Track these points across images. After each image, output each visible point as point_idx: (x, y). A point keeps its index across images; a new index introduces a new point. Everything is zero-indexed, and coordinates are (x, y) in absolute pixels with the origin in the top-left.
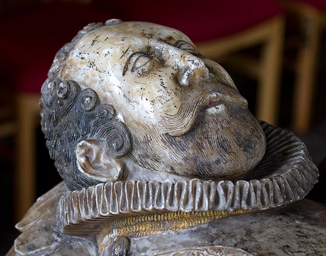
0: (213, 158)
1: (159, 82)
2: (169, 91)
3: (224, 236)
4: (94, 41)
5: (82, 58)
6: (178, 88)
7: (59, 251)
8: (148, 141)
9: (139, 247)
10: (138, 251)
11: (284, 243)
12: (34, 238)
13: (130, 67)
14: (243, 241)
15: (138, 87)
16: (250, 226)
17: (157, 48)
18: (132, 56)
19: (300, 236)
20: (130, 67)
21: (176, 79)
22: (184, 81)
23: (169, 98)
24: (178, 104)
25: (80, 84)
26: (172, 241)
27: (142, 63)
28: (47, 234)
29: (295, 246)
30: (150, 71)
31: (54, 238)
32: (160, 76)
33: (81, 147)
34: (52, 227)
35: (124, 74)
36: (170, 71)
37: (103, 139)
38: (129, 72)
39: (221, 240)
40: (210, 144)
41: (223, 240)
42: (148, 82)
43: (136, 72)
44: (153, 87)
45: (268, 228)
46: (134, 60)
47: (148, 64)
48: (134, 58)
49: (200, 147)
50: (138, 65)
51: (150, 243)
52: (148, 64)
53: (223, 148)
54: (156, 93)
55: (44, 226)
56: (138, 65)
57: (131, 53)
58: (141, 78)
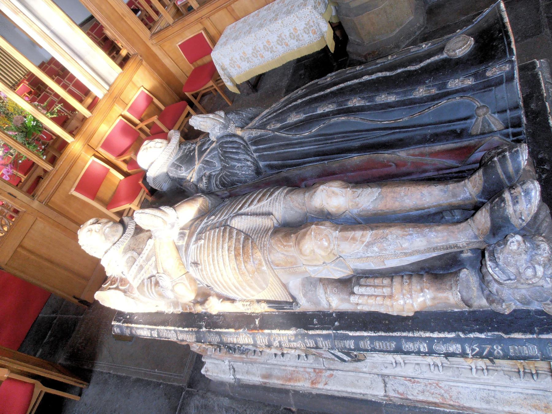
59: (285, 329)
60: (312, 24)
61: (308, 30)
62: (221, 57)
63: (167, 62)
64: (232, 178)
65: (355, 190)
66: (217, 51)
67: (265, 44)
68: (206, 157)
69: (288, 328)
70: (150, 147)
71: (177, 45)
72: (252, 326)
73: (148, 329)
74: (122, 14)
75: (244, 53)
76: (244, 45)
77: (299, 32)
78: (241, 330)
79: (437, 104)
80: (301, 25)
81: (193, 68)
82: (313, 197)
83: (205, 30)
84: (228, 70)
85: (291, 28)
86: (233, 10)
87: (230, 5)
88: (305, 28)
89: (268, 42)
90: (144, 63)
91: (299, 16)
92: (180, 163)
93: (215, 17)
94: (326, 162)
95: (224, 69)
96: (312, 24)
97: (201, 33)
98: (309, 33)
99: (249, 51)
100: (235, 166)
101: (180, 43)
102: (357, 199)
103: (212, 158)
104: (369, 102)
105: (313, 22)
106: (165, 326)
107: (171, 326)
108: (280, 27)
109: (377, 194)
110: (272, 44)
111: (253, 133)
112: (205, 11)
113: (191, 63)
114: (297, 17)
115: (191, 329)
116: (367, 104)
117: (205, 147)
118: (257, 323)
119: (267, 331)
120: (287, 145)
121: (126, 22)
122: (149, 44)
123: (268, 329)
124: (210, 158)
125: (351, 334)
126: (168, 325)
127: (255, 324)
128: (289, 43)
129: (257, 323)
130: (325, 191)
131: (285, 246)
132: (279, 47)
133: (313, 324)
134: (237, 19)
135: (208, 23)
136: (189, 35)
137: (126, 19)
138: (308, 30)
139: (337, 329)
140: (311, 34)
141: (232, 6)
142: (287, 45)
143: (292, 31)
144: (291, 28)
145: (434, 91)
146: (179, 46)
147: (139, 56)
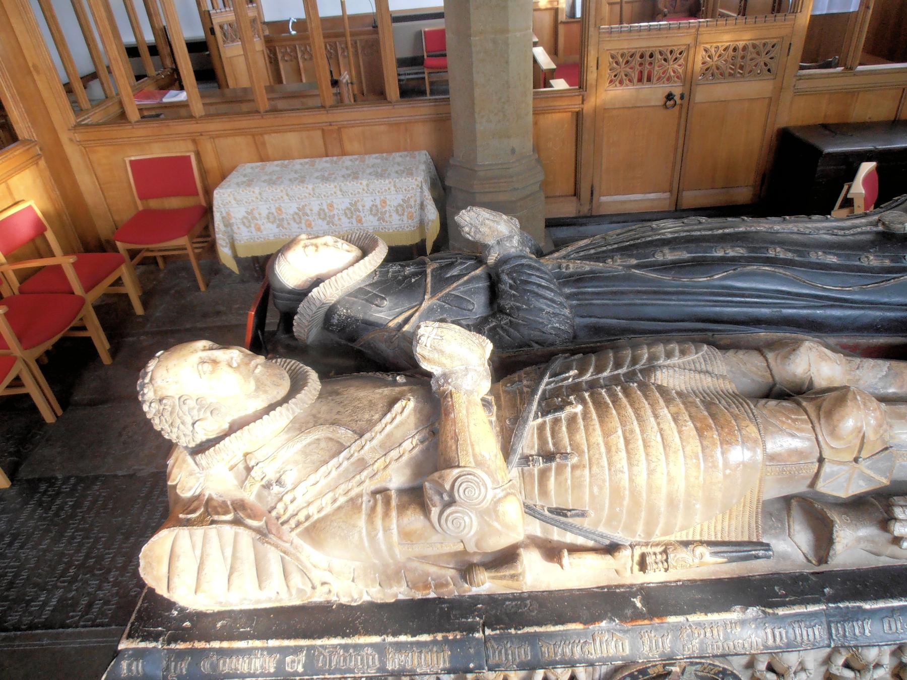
0: (275, 393)
11: (335, 411)
13: (201, 372)
14: (316, 422)
22: (235, 365)
27: (207, 367)
29: (342, 410)
38: (203, 375)
59: (719, 611)
60: (412, 203)
61: (404, 210)
62: (233, 202)
63: (85, 182)
64: (525, 331)
65: (849, 358)
66: (229, 190)
67: (325, 207)
68: (454, 289)
69: (727, 608)
70: (325, 244)
71: (127, 160)
72: (629, 612)
73: (271, 651)
74: (34, 66)
75: (279, 209)
76: (286, 197)
77: (387, 208)
78: (604, 624)
79: (894, 278)
80: (394, 199)
81: (141, 208)
82: (792, 357)
83: (198, 154)
84: (235, 227)
85: (378, 198)
86: (264, 144)
87: (261, 134)
88: (400, 205)
89: (331, 206)
90: (42, 163)
91: (398, 185)
92: (381, 291)
93: (226, 143)
94: (710, 334)
95: (228, 224)
96: (412, 203)
97: (189, 157)
98: (403, 214)
99: (291, 208)
100: (542, 310)
101: (133, 158)
102: (858, 372)
103: (470, 292)
104: (798, 256)
105: (415, 201)
106: (344, 635)
107: (368, 633)
108: (361, 191)
109: (886, 369)
110: (335, 212)
111: (571, 266)
112: (215, 126)
113: (142, 197)
114: (395, 186)
115: (439, 636)
116: (796, 258)
117: (455, 272)
118: (639, 605)
119: (672, 619)
120: (655, 293)
121: (34, 81)
122: (64, 137)
123: (676, 614)
124: (465, 292)
125: (867, 606)
126: (355, 632)
127: (634, 606)
128: (364, 220)
129: (639, 605)
130: (814, 350)
131: (794, 420)
132: (344, 220)
133: (777, 596)
134: (263, 158)
135: (208, 148)
136: (157, 151)
137: (36, 77)
138: (404, 210)
139: (835, 599)
140: (405, 218)
141: (266, 137)
142: (360, 221)
143: (378, 202)
144: (378, 198)
145: (887, 263)
146: (131, 162)
147: (37, 148)
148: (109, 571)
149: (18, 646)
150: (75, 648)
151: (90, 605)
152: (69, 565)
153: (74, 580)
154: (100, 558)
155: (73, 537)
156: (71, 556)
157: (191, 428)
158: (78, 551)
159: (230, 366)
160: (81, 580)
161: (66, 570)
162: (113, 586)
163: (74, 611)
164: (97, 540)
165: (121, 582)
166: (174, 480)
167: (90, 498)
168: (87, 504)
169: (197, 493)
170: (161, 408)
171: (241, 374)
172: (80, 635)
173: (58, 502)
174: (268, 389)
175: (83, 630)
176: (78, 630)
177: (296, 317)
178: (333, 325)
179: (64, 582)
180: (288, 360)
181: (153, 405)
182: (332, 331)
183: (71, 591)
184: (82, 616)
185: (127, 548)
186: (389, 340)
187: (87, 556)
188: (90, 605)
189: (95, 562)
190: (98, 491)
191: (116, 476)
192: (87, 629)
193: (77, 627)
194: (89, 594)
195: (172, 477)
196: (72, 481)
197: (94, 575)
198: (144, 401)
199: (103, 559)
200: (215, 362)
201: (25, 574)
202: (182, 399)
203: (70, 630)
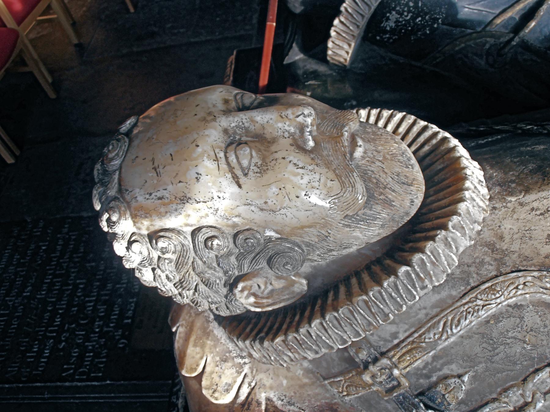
1: (291, 167)
2: (310, 168)
3: (472, 269)
4: (155, 169)
5: (160, 198)
6: (312, 156)
7: (257, 370)
8: (327, 237)
9: (383, 336)
10: (386, 340)
12: (220, 377)
13: (239, 173)
15: (274, 189)
16: (482, 238)
17: (233, 125)
18: (226, 158)
19: (541, 214)
20: (239, 173)
21: (299, 146)
23: (317, 176)
24: (331, 175)
25: (180, 228)
26: (420, 310)
27: (247, 156)
28: (230, 364)
30: (264, 159)
31: (240, 363)
32: (284, 158)
33: (242, 291)
34: (227, 354)
35: (240, 186)
36: (285, 142)
37: (260, 266)
39: (475, 275)
40: (394, 191)
41: (477, 274)
42: (280, 176)
43: (251, 173)
44: (292, 178)
45: (499, 226)
46: (235, 161)
47: (254, 154)
48: (232, 158)
49: (388, 203)
50: (245, 163)
51: (395, 326)
52: (254, 154)
53: (404, 183)
54: (301, 182)
55: (218, 359)
56: (245, 163)
57: (222, 155)
58: (266, 177)
148: (93, 321)
149: (23, 399)
150: (76, 403)
151: (81, 357)
152: (54, 313)
153: (61, 330)
154: (82, 306)
155: (52, 284)
156: (54, 304)
157: (224, 291)
158: (60, 299)
159: (300, 148)
160: (68, 328)
161: (52, 319)
162: (100, 337)
163: (68, 364)
164: (76, 286)
165: (108, 332)
166: (194, 370)
167: (61, 242)
168: (59, 248)
169: (243, 397)
170: (155, 254)
171: (328, 165)
172: (78, 390)
173: (33, 246)
174: (391, 196)
175: (79, 384)
176: (75, 384)
177: (336, 22)
178: (385, 32)
179: (52, 332)
180: (386, 113)
181: (135, 247)
182: (381, 44)
183: (60, 342)
184: (75, 370)
185: (106, 295)
186: (499, 50)
187: (70, 305)
188: (81, 357)
189: (77, 311)
190: (67, 233)
191: (82, 218)
192: (84, 384)
193: (72, 381)
194: (78, 346)
195: (188, 362)
196: (41, 224)
197: (79, 325)
198: (114, 236)
199: (85, 308)
200: (262, 141)
201: (15, 322)
202: (201, 238)
203: (67, 384)
